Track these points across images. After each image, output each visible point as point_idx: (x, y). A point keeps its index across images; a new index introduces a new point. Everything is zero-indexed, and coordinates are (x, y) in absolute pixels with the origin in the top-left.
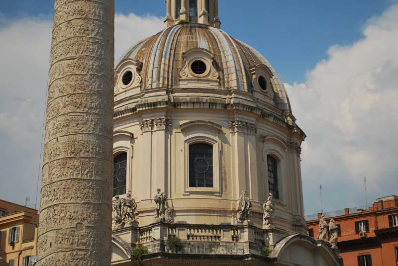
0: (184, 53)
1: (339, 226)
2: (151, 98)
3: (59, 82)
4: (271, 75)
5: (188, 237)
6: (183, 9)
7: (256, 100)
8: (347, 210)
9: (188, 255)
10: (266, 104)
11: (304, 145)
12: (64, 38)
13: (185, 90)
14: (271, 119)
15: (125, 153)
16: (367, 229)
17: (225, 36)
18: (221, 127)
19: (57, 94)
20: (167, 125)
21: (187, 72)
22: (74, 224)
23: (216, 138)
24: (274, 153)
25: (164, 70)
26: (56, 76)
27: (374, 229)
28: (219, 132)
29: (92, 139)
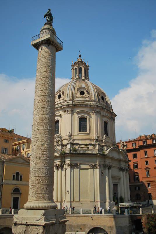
0: (77, 89)
1: (127, 144)
2: (67, 103)
3: (38, 98)
4: (105, 96)
5: (79, 148)
7: (101, 104)
8: (130, 139)
9: (78, 153)
10: (104, 105)
11: (116, 119)
12: (39, 84)
13: (78, 101)
14: (105, 110)
15: (59, 121)
16: (136, 146)
17: (91, 83)
18: (89, 112)
19: (37, 102)
20: (72, 112)
21: (79, 95)
22: (42, 143)
24: (106, 121)
25: (71, 94)
26: (37, 96)
27: (138, 145)
28: (89, 114)
29: (48, 116)
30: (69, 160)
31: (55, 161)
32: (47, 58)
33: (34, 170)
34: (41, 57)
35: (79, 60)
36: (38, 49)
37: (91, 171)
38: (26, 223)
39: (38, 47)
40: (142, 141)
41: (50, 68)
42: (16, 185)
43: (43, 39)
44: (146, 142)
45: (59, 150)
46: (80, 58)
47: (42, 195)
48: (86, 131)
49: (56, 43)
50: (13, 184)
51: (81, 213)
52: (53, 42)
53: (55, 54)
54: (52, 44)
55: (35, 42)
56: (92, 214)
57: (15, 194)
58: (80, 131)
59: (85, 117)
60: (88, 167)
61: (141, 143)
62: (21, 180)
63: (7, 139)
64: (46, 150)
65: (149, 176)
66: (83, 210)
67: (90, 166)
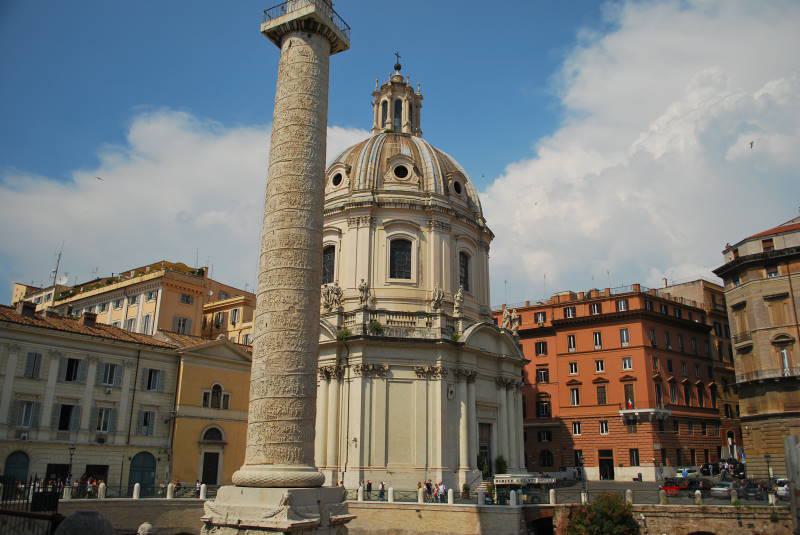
4: (465, 181)
5: (388, 322)
6: (388, 119)
7: (452, 203)
10: (459, 206)
12: (280, 142)
14: (465, 220)
15: (333, 247)
16: (545, 320)
17: (426, 145)
19: (274, 192)
20: (371, 222)
21: (391, 175)
22: (287, 307)
23: (415, 236)
26: (274, 176)
28: (418, 230)
29: (304, 233)
30: (361, 354)
31: (321, 358)
32: (304, 69)
33: (262, 380)
34: (287, 68)
35: (395, 80)
36: (279, 45)
37: (419, 385)
38: (239, 521)
39: (280, 39)
40: (562, 309)
41: (311, 98)
42: (213, 421)
43: (295, 16)
44: (574, 311)
45: (333, 327)
46: (397, 73)
47: (283, 448)
48: (409, 278)
49: (331, 27)
50: (202, 418)
51: (390, 500)
52: (323, 26)
53: (327, 59)
54: (320, 33)
55: (272, 24)
56: (420, 501)
57: (208, 444)
58: (392, 276)
59: (409, 238)
60: (411, 374)
61: (559, 315)
62: (226, 407)
63: (187, 293)
64: (296, 325)
65: (578, 403)
66: (394, 492)
67: (417, 373)
